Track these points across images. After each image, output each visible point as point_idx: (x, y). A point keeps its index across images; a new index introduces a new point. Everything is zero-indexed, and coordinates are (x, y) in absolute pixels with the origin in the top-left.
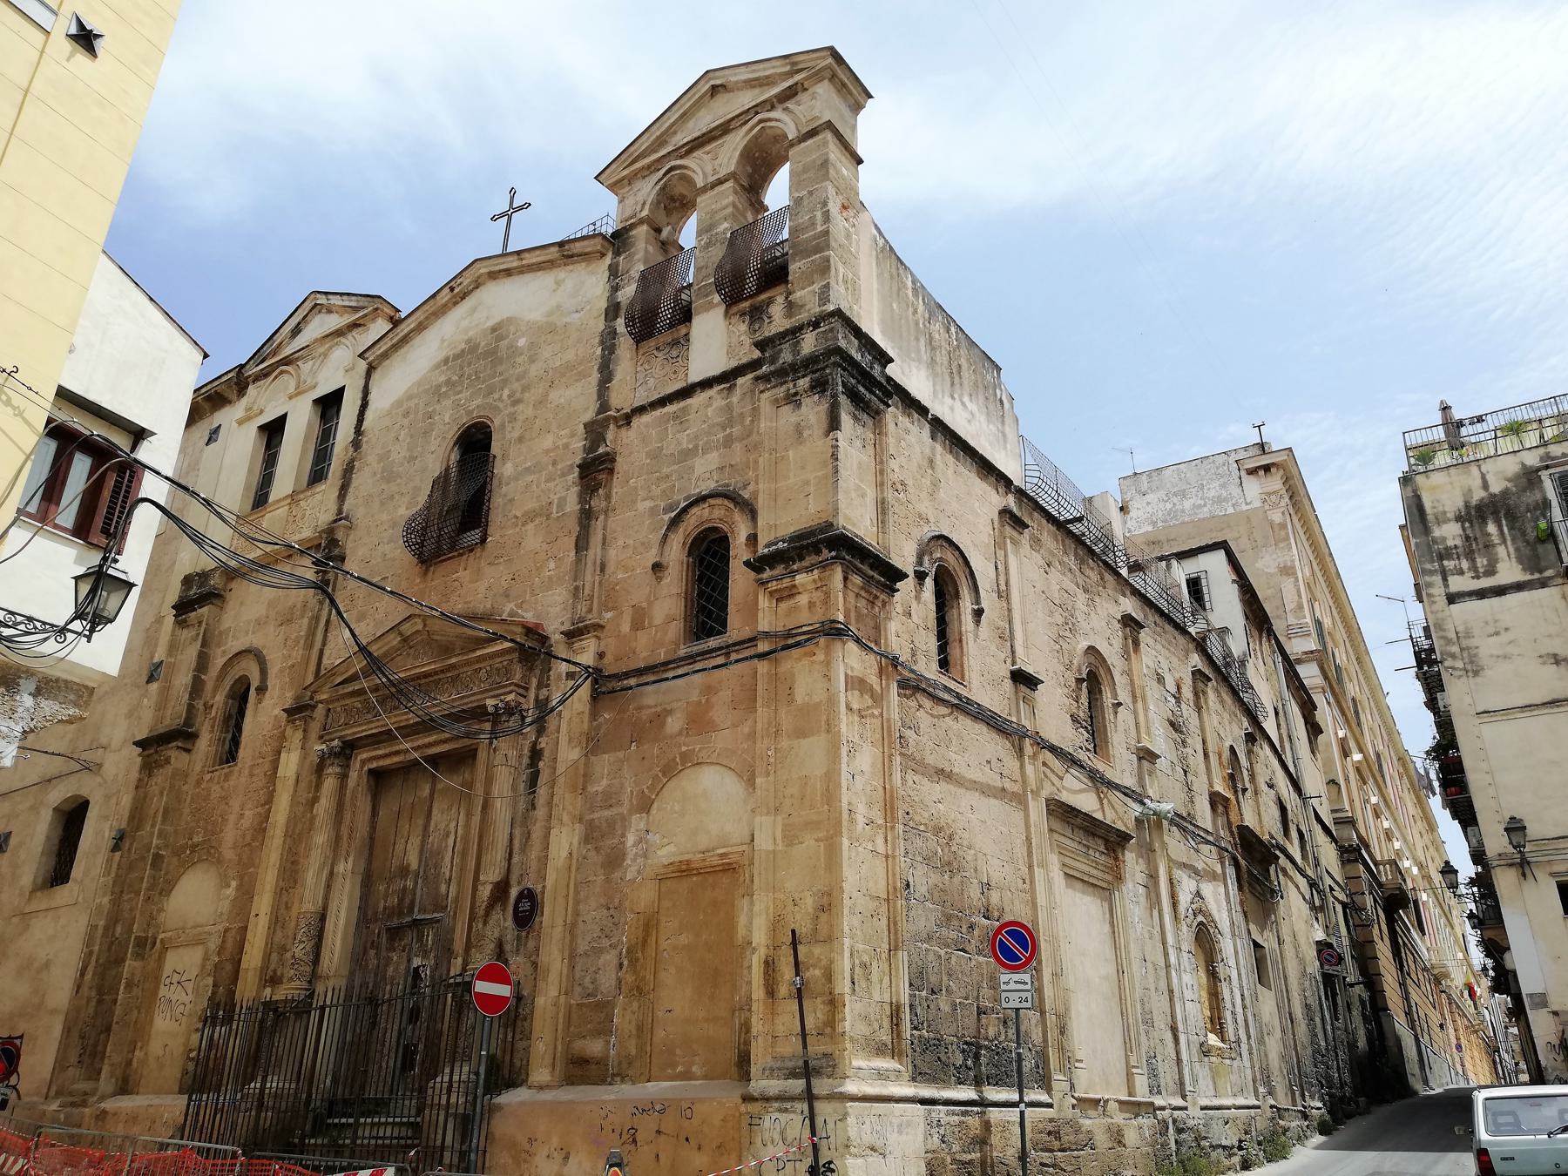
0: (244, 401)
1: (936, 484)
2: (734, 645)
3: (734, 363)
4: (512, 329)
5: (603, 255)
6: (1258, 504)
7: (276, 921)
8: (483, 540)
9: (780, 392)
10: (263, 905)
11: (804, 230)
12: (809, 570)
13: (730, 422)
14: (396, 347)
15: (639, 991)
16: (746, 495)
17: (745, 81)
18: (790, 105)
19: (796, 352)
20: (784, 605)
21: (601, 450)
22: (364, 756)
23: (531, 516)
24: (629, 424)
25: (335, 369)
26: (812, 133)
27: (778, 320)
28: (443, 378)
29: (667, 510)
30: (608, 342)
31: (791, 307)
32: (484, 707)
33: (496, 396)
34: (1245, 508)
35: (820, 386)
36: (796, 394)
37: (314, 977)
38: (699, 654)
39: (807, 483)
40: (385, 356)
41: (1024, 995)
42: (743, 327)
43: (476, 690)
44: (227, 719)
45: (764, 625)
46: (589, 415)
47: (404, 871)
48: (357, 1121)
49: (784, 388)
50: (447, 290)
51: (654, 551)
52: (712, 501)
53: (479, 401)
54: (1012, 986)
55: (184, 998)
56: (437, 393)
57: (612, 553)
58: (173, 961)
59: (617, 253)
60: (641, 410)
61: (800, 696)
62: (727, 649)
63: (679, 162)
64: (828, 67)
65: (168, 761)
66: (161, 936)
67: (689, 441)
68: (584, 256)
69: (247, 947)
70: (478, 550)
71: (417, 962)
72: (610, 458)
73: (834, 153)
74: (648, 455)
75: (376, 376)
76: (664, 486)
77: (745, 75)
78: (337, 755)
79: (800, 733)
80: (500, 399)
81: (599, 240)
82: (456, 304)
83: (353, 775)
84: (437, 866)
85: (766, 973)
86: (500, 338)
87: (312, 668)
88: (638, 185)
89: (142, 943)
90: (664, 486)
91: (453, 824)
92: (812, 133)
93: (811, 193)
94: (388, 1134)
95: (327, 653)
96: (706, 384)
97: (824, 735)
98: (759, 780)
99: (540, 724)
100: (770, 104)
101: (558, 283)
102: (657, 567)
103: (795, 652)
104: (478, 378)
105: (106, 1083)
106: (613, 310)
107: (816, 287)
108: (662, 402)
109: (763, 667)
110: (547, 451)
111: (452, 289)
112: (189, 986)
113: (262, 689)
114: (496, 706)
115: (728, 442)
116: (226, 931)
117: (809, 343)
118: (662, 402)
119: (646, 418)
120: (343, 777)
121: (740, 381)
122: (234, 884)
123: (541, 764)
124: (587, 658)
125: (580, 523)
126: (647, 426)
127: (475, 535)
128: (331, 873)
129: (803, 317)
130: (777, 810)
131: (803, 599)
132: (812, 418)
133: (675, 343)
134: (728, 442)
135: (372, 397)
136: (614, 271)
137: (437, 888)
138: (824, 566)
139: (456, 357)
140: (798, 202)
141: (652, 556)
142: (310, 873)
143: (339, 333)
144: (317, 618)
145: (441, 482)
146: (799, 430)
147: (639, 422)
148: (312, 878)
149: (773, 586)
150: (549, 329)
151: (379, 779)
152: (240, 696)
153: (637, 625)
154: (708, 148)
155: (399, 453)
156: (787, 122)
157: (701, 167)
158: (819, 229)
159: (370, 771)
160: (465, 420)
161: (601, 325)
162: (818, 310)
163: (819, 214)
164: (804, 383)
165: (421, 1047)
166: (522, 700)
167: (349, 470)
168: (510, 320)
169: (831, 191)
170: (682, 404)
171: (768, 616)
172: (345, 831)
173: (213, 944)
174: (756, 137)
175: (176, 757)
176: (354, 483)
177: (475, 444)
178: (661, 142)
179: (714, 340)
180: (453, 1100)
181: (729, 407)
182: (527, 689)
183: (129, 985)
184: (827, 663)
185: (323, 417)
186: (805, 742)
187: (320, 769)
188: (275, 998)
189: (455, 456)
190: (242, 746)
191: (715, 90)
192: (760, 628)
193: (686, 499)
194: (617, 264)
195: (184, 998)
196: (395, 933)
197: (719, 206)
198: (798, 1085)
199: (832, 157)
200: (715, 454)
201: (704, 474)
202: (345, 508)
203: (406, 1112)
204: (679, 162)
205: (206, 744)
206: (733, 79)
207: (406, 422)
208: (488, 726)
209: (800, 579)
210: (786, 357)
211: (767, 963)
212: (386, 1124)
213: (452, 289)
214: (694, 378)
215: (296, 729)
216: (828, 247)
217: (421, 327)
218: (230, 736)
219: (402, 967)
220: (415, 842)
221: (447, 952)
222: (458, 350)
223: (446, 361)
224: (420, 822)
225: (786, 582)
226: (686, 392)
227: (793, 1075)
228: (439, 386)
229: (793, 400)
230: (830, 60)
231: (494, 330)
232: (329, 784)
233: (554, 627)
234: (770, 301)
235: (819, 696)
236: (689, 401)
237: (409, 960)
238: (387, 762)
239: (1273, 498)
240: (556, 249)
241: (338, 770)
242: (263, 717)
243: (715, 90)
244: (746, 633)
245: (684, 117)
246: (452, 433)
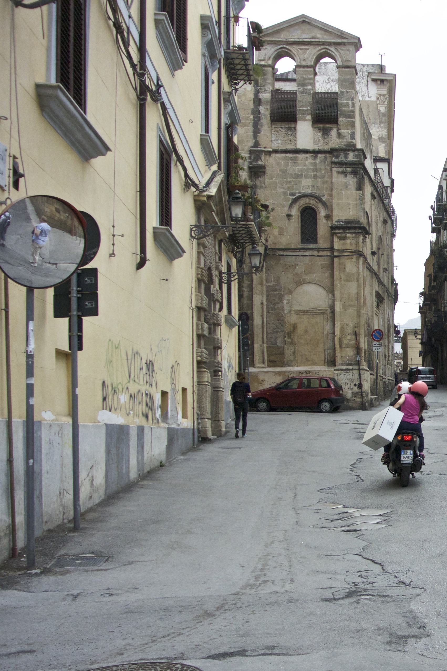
6: (374, 99)
9: (341, 170)
15: (292, 343)
16: (324, 199)
19: (346, 157)
29: (292, 194)
34: (367, 99)
36: (346, 172)
38: (307, 249)
51: (286, 209)
60: (276, 151)
61: (348, 270)
62: (319, 250)
64: (356, 43)
67: (299, 171)
79: (348, 281)
97: (356, 282)
102: (289, 216)
121: (319, 155)
126: (279, 158)
131: (348, 241)
132: (351, 182)
133: (289, 129)
147: (273, 155)
149: (339, 235)
153: (281, 234)
164: (349, 170)
170: (294, 155)
179: (306, 134)
186: (350, 283)
191: (304, 22)
193: (299, 193)
198: (356, 367)
209: (348, 235)
210: (342, 158)
211: (339, 339)
225: (343, 235)
227: (355, 364)
229: (345, 174)
230: (357, 41)
235: (354, 271)
239: (382, 97)
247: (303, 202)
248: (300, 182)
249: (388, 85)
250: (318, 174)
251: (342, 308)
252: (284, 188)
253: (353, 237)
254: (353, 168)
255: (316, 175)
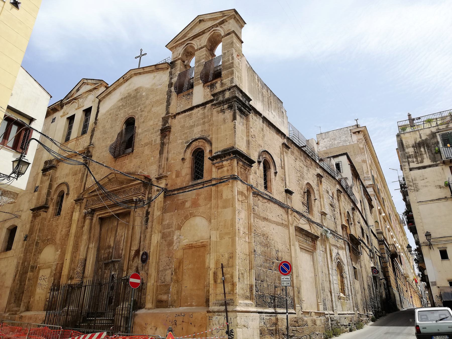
0: (63, 110)
1: (264, 136)
2: (206, 182)
3: (205, 101)
4: (141, 90)
5: (168, 69)
6: (356, 142)
7: (72, 261)
8: (132, 151)
9: (219, 109)
10: (68, 257)
11: (226, 62)
12: (227, 160)
13: (204, 117)
14: (107, 95)
15: (177, 281)
16: (209, 138)
17: (209, 19)
18: (222, 26)
19: (224, 97)
20: (219, 170)
21: (167, 125)
22: (98, 213)
23: (146, 144)
24: (175, 118)
25: (89, 101)
26: (229, 34)
27: (218, 88)
28: (121, 104)
29: (186, 143)
30: (169, 94)
31: (222, 84)
32: (133, 199)
33: (136, 109)
34: (352, 143)
35: (230, 107)
36: (224, 109)
37: (83, 277)
38: (195, 185)
39: (227, 135)
40: (104, 97)
41: (288, 282)
42: (208, 90)
43: (130, 194)
44: (57, 203)
45: (214, 176)
46: (163, 115)
47: (109, 247)
48: (95, 319)
49: (220, 108)
50: (122, 78)
51: (182, 155)
52: (199, 140)
53: (131, 111)
54: (285, 280)
55: (45, 283)
56: (119, 108)
57: (170, 155)
58: (42, 273)
59: (172, 68)
60: (179, 114)
61: (224, 197)
62: (203, 183)
63: (190, 42)
64: (233, 15)
65: (40, 215)
66: (38, 265)
67: (193, 123)
68: (162, 69)
69: (63, 269)
70: (131, 154)
71: (113, 273)
72: (169, 128)
73: (235, 40)
74: (180, 127)
75: (101, 103)
76: (185, 136)
77: (209, 17)
78: (90, 213)
79: (224, 207)
80: (137, 110)
81: (166, 64)
82: (125, 82)
83: (95, 219)
84: (119, 245)
85: (214, 276)
86: (137, 93)
87: (82, 188)
88: (178, 48)
89: (33, 268)
90: (185, 136)
91: (124, 233)
92: (229, 34)
93: (228, 51)
94: (105, 322)
95: (87, 183)
96: (198, 106)
97: (231, 208)
98: (212, 221)
99: (149, 205)
100: (216, 25)
101: (155, 77)
102: (183, 159)
103: (223, 184)
104: (131, 104)
105: (22, 308)
106: (170, 85)
107: (229, 79)
108: (185, 111)
109: (214, 188)
110: (151, 126)
111: (124, 78)
112: (47, 280)
113: (68, 194)
114: (136, 199)
115: (204, 123)
116: (57, 264)
117: (227, 95)
118: (185, 111)
119: (180, 116)
120: (92, 220)
121: (207, 105)
122: (60, 250)
123: (149, 216)
124: (163, 185)
125: (161, 147)
126: (180, 119)
127: (130, 150)
128: (88, 247)
129: (226, 87)
130: (217, 229)
131: (225, 169)
132: (228, 117)
133: (189, 94)
134: (204, 123)
135: (100, 110)
136: (171, 73)
137: (119, 252)
138: (231, 159)
139: (125, 98)
140: (224, 54)
141: (181, 156)
142: (82, 247)
143: (90, 91)
144: (84, 174)
145: (120, 134)
146: (224, 120)
147: (178, 117)
148: (82, 249)
149: (217, 165)
150: (152, 90)
151: (102, 220)
152: (61, 196)
154: (198, 38)
155: (108, 126)
156: (221, 31)
157: (196, 44)
158: (231, 62)
159: (99, 218)
160: (127, 116)
161: (167, 89)
162: (230, 85)
163: (230, 58)
164: (226, 106)
165: (114, 297)
166: (144, 197)
167: (93, 131)
168: (141, 87)
169: (234, 51)
170: (191, 112)
171: (215, 174)
172: (92, 235)
173: (54, 268)
174: (212, 35)
175: (43, 214)
176: (95, 135)
177: (130, 123)
178: (185, 36)
179: (200, 94)
180: (123, 312)
181: (204, 113)
182: (145, 194)
183: (29, 280)
184: (232, 187)
185: (86, 115)
186: (226, 210)
187: (85, 217)
188: (72, 283)
189: (124, 127)
190: (62, 210)
191: (200, 21)
192: (213, 177)
193: (191, 140)
194: (172, 71)
195: (45, 283)
196: (107, 265)
197: (201, 55)
198: (223, 308)
199: (234, 41)
200: (200, 127)
201: (197, 132)
202: (92, 142)
203: (110, 316)
204: (190, 42)
205: (51, 210)
206: (206, 18)
207: (110, 117)
208: (134, 205)
209: (225, 163)
210: (221, 99)
211: (214, 273)
212: (104, 319)
213: (124, 78)
214: (194, 104)
215: (78, 206)
216: (233, 67)
217: (114, 89)
218: (58, 208)
219: (109, 274)
220: (112, 238)
221: (122, 270)
222: (125, 96)
223: (122, 99)
224: (114, 232)
225: (221, 164)
226: (192, 109)
227: (221, 305)
228: (120, 106)
229: (223, 111)
230: (234, 13)
231: (136, 90)
232: (87, 222)
233: (153, 177)
234: (216, 83)
235: (230, 197)
236: (193, 111)
237: (111, 272)
238: (104, 215)
239: (360, 140)
240: (154, 67)
241: (90, 217)
242: (68, 202)
243: (200, 21)
244: (209, 178)
245: (191, 29)
246: (124, 120)
247: (195, 145)
248: (193, 131)
249: (363, 133)
250: (206, 120)
251: (218, 237)
252: (182, 139)
253: (229, 164)
254: (229, 103)
255: (204, 121)
